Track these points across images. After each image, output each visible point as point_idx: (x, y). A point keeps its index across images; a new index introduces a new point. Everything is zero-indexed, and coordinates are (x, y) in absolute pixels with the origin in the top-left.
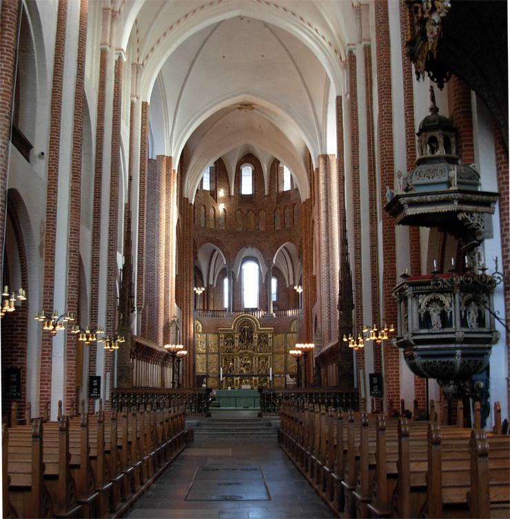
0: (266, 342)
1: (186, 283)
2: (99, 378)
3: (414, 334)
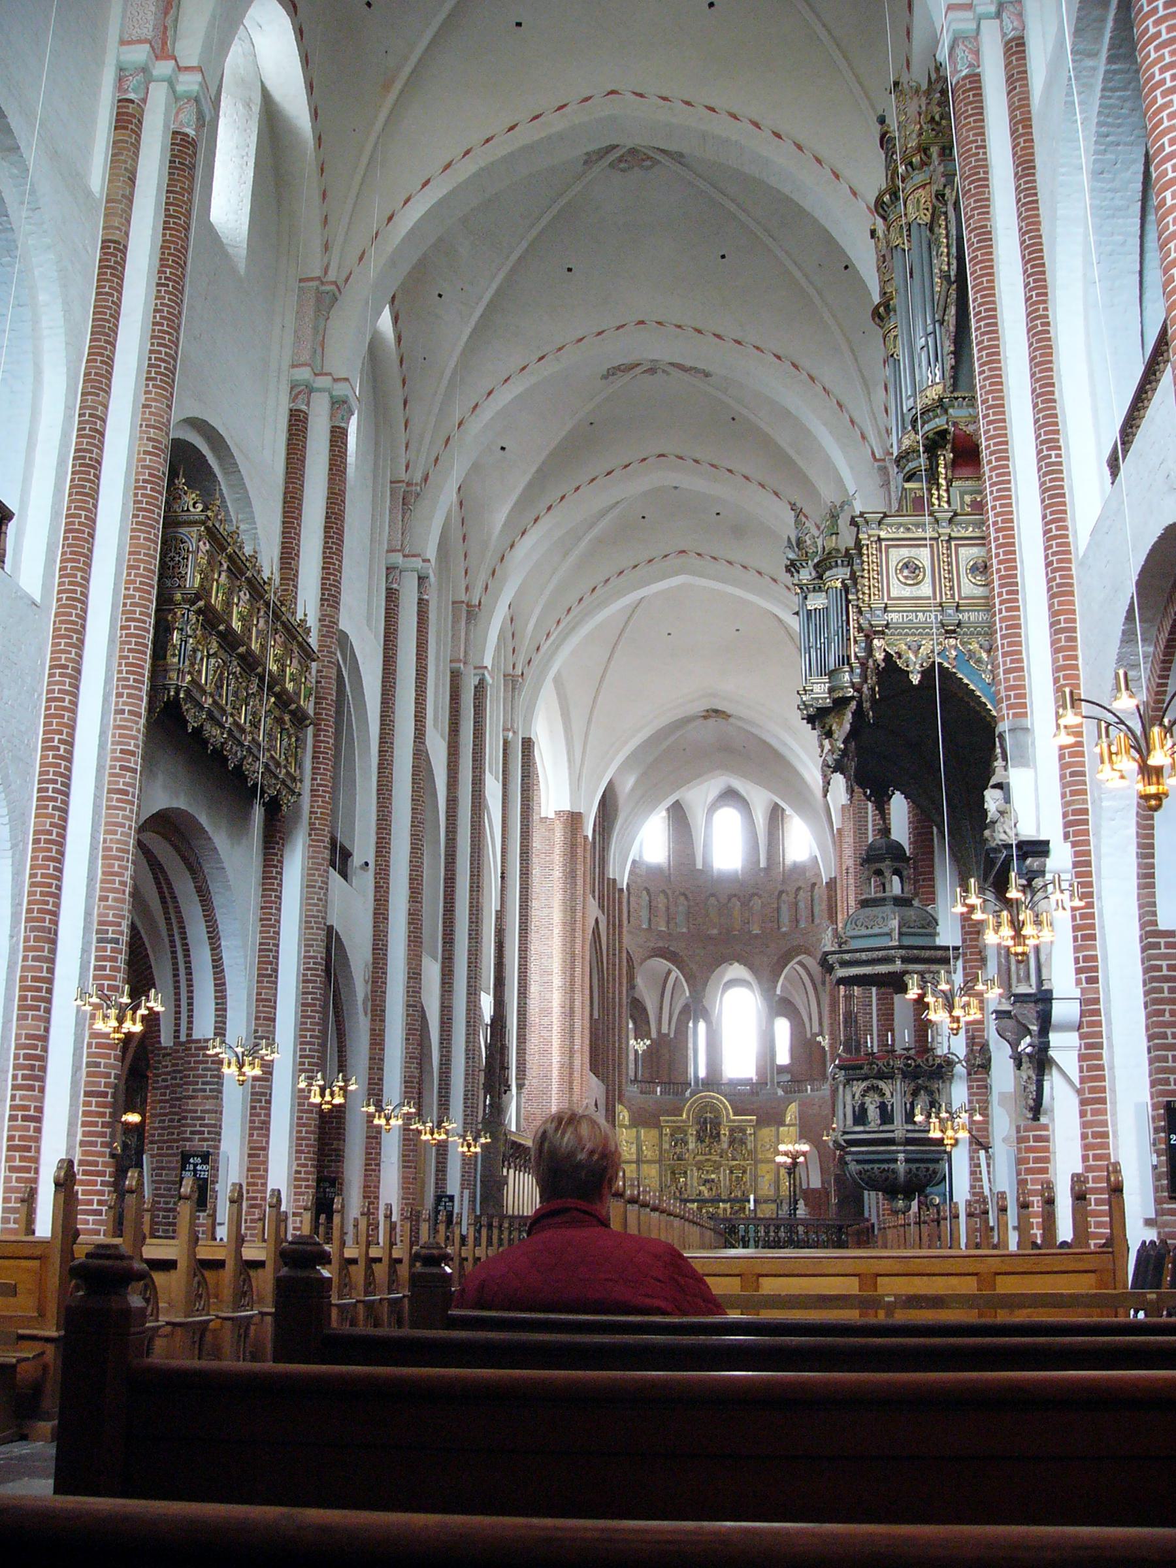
0: (743, 1142)
1: (614, 1035)
2: (451, 1198)
3: (845, 1133)
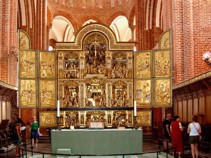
1: (40, 37)
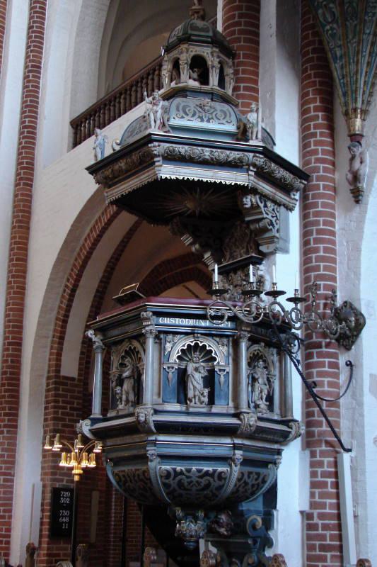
3: (156, 412)
